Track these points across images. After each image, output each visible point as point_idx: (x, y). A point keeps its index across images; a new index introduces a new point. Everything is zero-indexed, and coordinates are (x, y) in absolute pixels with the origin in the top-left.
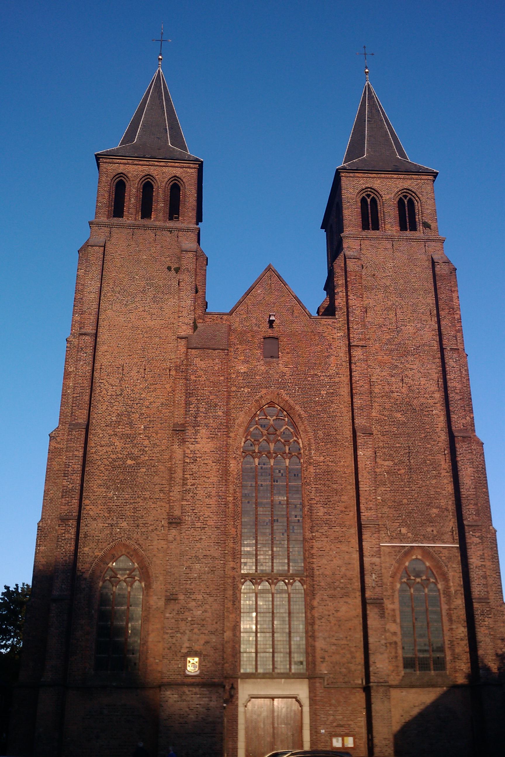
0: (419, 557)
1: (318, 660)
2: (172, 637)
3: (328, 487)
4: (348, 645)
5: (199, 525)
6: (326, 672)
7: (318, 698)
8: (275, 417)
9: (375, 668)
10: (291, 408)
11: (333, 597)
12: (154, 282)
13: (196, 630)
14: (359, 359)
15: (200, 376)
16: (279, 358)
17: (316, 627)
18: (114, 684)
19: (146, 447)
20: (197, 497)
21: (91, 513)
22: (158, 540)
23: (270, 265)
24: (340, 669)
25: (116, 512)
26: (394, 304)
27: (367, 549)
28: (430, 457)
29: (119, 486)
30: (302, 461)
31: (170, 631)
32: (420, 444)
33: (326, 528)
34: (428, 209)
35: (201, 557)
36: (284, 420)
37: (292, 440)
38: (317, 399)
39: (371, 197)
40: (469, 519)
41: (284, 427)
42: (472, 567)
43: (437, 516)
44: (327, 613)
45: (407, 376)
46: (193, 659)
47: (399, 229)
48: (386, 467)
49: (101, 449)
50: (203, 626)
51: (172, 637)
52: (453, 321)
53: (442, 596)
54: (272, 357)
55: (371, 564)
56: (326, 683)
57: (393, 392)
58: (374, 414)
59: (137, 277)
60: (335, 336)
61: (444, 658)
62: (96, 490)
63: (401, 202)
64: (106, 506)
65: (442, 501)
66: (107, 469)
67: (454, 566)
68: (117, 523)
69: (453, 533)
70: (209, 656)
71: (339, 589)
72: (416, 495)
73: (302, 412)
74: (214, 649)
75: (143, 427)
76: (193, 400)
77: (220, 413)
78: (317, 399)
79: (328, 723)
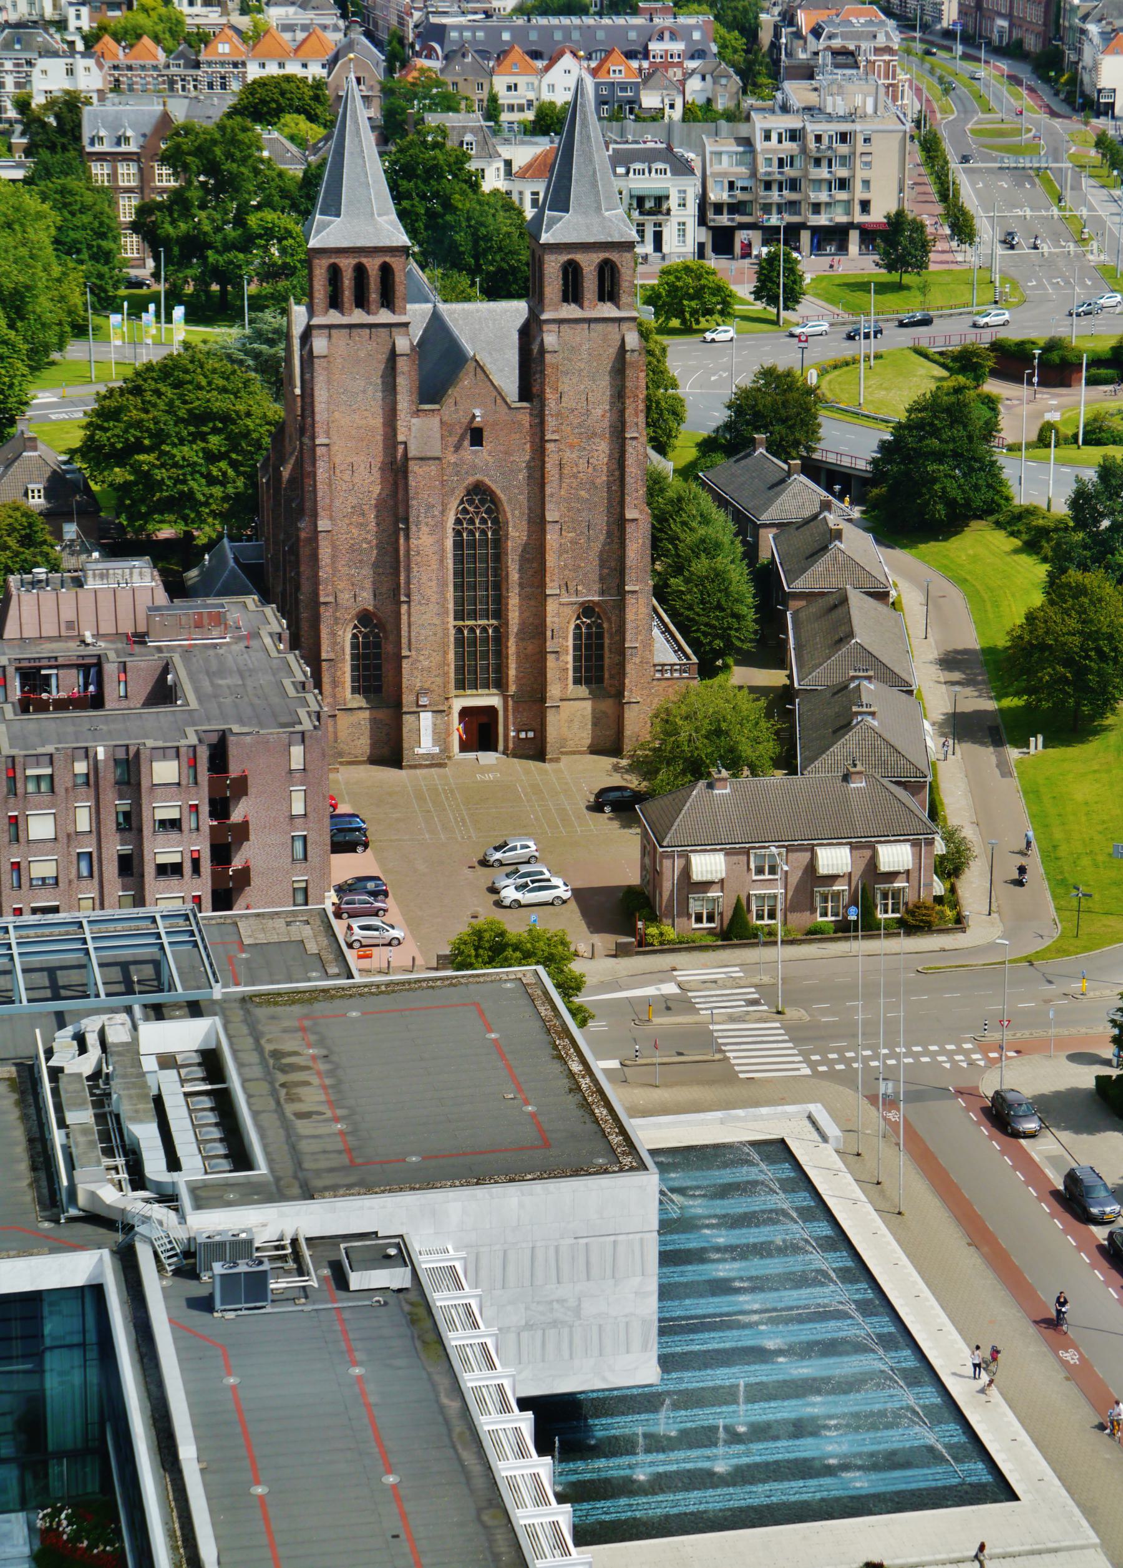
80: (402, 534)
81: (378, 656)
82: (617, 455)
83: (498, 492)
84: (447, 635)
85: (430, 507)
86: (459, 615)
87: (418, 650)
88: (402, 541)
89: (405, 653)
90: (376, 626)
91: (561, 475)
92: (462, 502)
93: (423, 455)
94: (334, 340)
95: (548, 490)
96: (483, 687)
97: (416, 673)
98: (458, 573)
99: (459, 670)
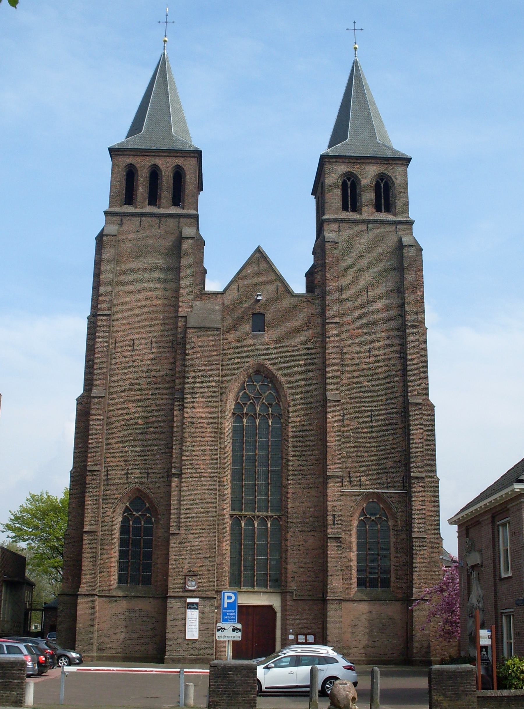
0: (375, 500)
1: (289, 579)
2: (176, 561)
3: (303, 443)
4: (313, 568)
5: (195, 475)
6: (295, 588)
7: (288, 607)
8: (260, 383)
9: (332, 586)
10: (274, 376)
11: (303, 531)
12: (159, 264)
13: (194, 556)
14: (332, 334)
15: (197, 352)
16: (264, 332)
17: (289, 554)
18: (133, 594)
19: (153, 410)
20: (194, 453)
21: (111, 464)
22: (164, 485)
23: (259, 247)
24: (306, 586)
25: (131, 463)
26: (366, 282)
27: (330, 495)
28: (389, 418)
29: (132, 442)
30: (282, 421)
31: (175, 557)
32: (381, 407)
33: (300, 477)
34: (401, 192)
35: (198, 501)
36: (268, 385)
37: (275, 403)
38: (296, 368)
39: (351, 180)
40: (415, 472)
41: (268, 392)
42: (414, 509)
43: (392, 467)
44: (298, 543)
45: (374, 347)
46: (192, 578)
47: (375, 211)
48: (351, 427)
49: (117, 411)
50: (199, 553)
51: (176, 561)
52: (415, 299)
53: (391, 531)
54: (259, 331)
55: (333, 507)
56: (294, 596)
57: (361, 362)
58: (344, 381)
59: (145, 261)
60: (313, 312)
61: (389, 579)
62: (114, 445)
63: (377, 186)
64: (122, 459)
65: (396, 455)
66: (122, 428)
67: (402, 507)
68: (132, 472)
69: (404, 481)
70: (204, 575)
71: (308, 525)
72: (375, 450)
73: (283, 380)
74: (208, 571)
75: (150, 393)
76: (191, 372)
77: (214, 384)
78: (296, 368)
79: (295, 625)
80: (176, 404)
81: (149, 543)
82: (398, 348)
83: (279, 376)
84: (222, 522)
85: (207, 377)
86: (237, 504)
87: (187, 528)
88: (176, 412)
89: (172, 530)
90: (148, 510)
91: (342, 363)
92: (243, 388)
93: (202, 326)
94: (124, 227)
95: (330, 372)
96: (259, 586)
97: (184, 552)
98: (237, 461)
99: (236, 563)
